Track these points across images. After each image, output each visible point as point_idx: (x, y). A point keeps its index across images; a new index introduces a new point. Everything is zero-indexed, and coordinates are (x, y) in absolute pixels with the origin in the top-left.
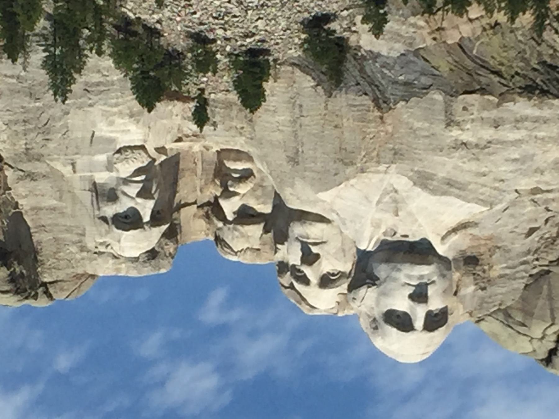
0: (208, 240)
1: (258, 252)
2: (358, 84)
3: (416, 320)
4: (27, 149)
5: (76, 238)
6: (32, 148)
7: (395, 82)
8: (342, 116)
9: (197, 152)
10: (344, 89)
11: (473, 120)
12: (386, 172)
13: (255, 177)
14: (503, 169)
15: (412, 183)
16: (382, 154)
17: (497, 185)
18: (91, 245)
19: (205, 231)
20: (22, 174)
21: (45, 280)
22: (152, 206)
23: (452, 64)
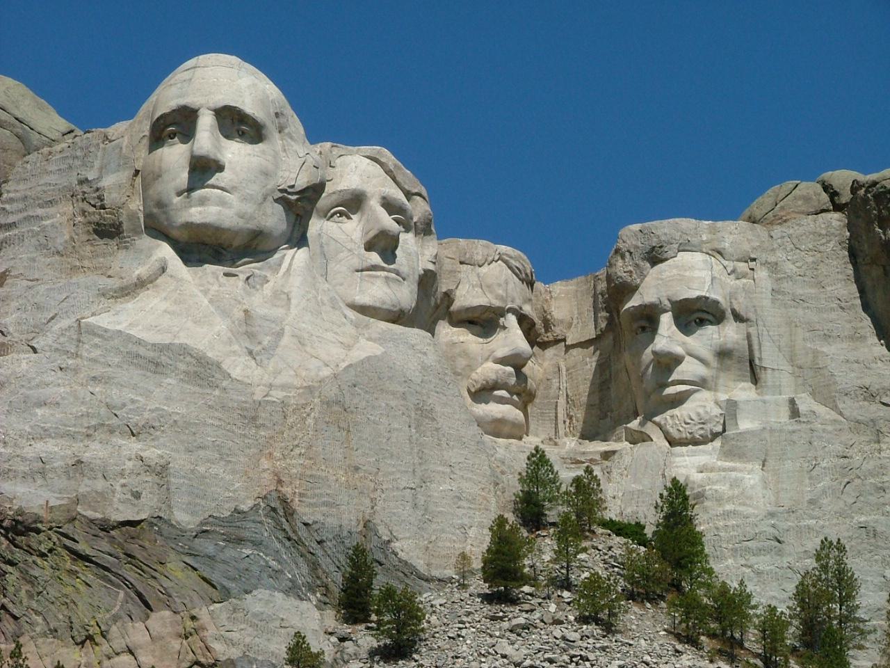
0: (547, 281)
1: (463, 259)
2: (319, 543)
3: (212, 126)
4: (879, 442)
5: (786, 286)
6: (869, 442)
7: (257, 544)
8: (348, 487)
9: (566, 435)
10: (345, 533)
11: (122, 475)
12: (271, 386)
13: (469, 391)
14: (62, 390)
15: (224, 366)
16: (278, 417)
17: (70, 362)
18: (762, 273)
19: (551, 297)
20: (885, 400)
21: (837, 215)
22: (657, 339)
23: (162, 574)
